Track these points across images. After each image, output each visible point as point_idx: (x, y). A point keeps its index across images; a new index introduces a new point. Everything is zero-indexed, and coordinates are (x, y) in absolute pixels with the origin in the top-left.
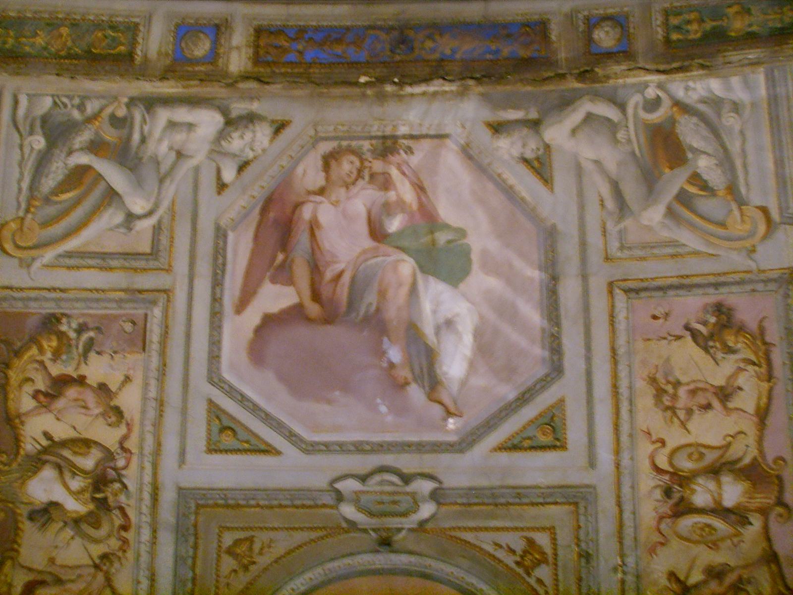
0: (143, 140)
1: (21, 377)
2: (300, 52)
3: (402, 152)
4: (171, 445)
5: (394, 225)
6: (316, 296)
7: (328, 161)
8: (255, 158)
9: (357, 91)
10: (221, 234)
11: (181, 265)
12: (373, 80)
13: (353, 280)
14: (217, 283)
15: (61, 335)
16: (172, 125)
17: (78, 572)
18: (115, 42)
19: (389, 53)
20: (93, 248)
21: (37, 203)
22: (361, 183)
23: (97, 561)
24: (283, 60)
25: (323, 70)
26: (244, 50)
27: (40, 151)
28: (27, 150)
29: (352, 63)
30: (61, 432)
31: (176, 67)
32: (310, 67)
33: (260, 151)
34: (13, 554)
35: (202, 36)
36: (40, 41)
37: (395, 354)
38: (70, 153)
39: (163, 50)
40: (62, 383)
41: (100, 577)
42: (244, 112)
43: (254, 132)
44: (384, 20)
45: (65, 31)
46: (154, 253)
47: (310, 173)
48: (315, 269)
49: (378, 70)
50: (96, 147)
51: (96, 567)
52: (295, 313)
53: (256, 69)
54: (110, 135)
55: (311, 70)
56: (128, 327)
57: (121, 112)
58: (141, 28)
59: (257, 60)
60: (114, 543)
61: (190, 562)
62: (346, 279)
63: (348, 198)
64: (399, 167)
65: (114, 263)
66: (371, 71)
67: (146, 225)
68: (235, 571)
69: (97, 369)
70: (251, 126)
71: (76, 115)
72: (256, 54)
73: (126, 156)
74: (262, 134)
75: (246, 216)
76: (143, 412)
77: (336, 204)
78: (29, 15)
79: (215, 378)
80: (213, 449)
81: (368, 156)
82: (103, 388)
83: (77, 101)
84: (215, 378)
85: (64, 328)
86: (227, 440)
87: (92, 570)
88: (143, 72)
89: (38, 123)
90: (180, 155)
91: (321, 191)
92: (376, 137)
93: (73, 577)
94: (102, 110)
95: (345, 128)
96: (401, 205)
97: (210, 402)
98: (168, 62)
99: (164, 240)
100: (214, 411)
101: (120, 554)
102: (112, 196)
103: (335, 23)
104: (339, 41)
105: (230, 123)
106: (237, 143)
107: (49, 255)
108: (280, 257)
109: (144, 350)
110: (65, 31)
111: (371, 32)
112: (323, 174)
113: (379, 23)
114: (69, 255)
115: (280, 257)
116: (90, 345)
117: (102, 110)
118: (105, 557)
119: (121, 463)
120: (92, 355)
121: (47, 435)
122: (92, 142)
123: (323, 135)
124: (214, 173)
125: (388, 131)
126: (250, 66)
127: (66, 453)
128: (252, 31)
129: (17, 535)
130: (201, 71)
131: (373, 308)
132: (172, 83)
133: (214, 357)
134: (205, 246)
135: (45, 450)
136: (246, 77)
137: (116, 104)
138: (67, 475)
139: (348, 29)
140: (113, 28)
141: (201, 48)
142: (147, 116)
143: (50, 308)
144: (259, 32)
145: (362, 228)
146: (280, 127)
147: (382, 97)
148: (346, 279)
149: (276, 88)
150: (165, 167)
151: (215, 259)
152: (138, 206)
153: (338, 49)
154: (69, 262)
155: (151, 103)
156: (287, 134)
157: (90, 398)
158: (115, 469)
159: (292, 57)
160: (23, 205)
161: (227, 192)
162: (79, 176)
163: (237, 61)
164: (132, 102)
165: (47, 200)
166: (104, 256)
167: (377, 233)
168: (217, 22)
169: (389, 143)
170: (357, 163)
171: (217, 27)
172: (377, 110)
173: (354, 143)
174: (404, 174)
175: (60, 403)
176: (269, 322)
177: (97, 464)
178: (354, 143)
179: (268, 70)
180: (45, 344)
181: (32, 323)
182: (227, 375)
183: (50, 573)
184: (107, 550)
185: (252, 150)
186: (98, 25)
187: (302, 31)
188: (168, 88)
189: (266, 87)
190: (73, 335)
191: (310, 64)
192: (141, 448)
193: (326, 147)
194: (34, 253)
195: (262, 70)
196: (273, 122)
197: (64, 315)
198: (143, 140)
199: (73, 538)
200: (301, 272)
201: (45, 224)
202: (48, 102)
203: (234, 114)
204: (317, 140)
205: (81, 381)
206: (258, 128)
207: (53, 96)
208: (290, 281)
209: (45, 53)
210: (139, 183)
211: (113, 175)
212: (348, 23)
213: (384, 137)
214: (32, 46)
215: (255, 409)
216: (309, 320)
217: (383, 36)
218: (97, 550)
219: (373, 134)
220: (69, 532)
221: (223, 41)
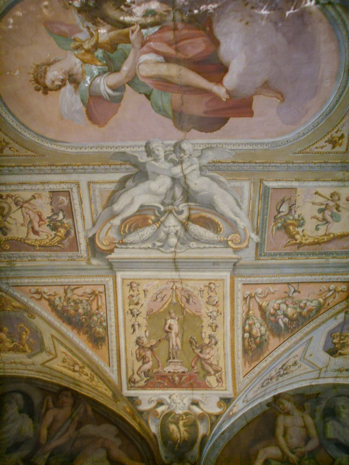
17: (25, 214)
23: (19, 207)
34: (22, 240)
41: (26, 205)
51: (21, 207)
60: (9, 200)
61: (10, 168)
68: (10, 148)
87: (23, 209)
93: (28, 216)
101: (14, 198)
118: (16, 204)
129: (14, 239)
183: (28, 225)
184: (13, 203)
199: (11, 217)
218: (14, 207)
220: (8, 219)
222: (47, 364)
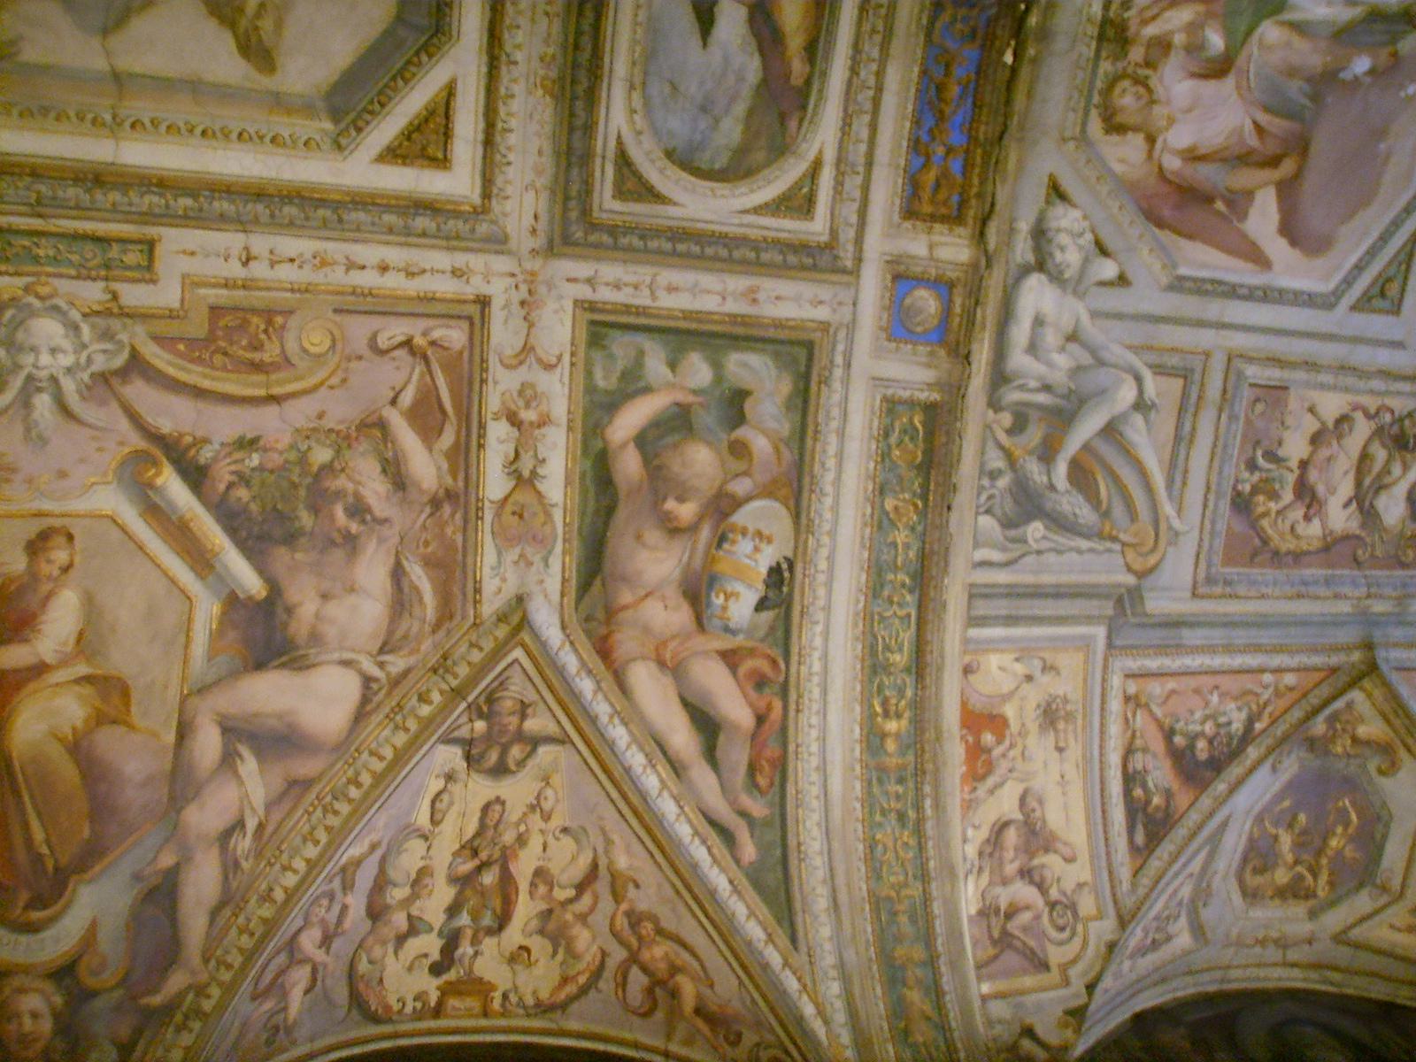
0: (1047, 388)
1: (1289, 537)
2: (950, 150)
3: (1126, 15)
4: (1384, 358)
5: (1216, 41)
6: (1274, 162)
7: (1115, 127)
8: (1093, 231)
9: (1025, 73)
10: (1179, 285)
11: (1206, 338)
12: (1013, 43)
13: (1267, 109)
14: (1232, 292)
15: (1255, 490)
16: (1033, 348)
18: (909, 431)
19: (975, 12)
20: (1167, 457)
21: (1107, 528)
22: (1153, 82)
24: (959, 179)
25: (984, 118)
26: (936, 238)
27: (1046, 527)
28: (1045, 545)
29: (978, 73)
30: (1346, 488)
31: (953, 341)
32: (976, 139)
33: (1086, 224)
35: (908, 301)
36: (901, 537)
37: (1361, 65)
38: (1052, 487)
39: (924, 360)
40: (1304, 491)
42: (1030, 242)
43: (1058, 230)
44: (921, 11)
45: (889, 504)
46: (1185, 374)
47: (1125, 154)
48: (1244, 159)
49: (999, 32)
50: (1047, 454)
52: (1287, 192)
53: (970, 221)
54: (1034, 434)
55: (981, 137)
56: (1260, 407)
57: (1006, 419)
58: (890, 392)
59: (956, 219)
62: (1263, 118)
63: (1168, 102)
64: (1145, 22)
65: (1187, 427)
66: (997, 43)
67: (1151, 384)
69: (1295, 447)
70: (1050, 234)
71: (1003, 482)
72: (944, 219)
73: (1063, 416)
74: (1065, 220)
75: (1163, 248)
76: (1347, 390)
77: (1171, 121)
78: (866, 555)
79: (1326, 303)
80: (1396, 310)
81: (1120, 65)
82: (1316, 440)
83: (986, 482)
84: (1326, 303)
85: (1247, 488)
86: (1393, 291)
88: (956, 390)
89: (1012, 533)
90: (1073, 337)
91: (1151, 140)
92: (1098, 51)
94: (1002, 447)
95: (1076, 95)
96: (1194, 28)
97: (1353, 308)
98: (942, 353)
99: (1174, 361)
100: (1363, 305)
102: (1111, 431)
103: (913, 90)
104: (940, 88)
105: (1041, 266)
106: (1069, 255)
107: (1168, 509)
108: (1220, 205)
109: (1286, 388)
110: (889, 504)
111: (937, 32)
112: (1130, 135)
113: (924, 21)
114: (1170, 483)
115: (1220, 205)
116: (1271, 456)
117: (1002, 447)
119: (1388, 418)
120: (1281, 453)
121: (1346, 505)
122: (1040, 459)
123: (1078, 129)
124: (1103, 290)
125: (1093, 31)
126: (960, 230)
127: (1367, 481)
128: (908, 224)
130: (963, 305)
131: (1307, 88)
132: (975, 347)
133: (1308, 300)
134: (1189, 305)
135: (1360, 508)
136: (981, 236)
137: (995, 426)
138: (1387, 480)
139: (924, 72)
140: (887, 435)
141: (927, 302)
142: (1016, 383)
143: (1225, 505)
144: (910, 213)
145: (1210, 86)
146: (1056, 192)
147: (1044, 34)
148: (1263, 118)
149: (1002, 195)
150: (1086, 359)
151: (1207, 293)
152: (1126, 394)
153: (954, 91)
154: (1178, 484)
155: (1000, 377)
156: (1068, 184)
157: (1324, 453)
158: (1392, 425)
159: (956, 166)
160: (1108, 544)
161: (1130, 275)
162: (1080, 475)
163: (954, 249)
164: (994, 404)
165: (1106, 515)
166: (1178, 438)
167: (1219, 68)
168: (889, 277)
169: (1111, 33)
170: (1126, 83)
171: (897, 277)
172: (1060, 44)
173: (1099, 84)
174: (1154, 18)
175: (1321, 489)
176: (1289, 229)
177: (1384, 445)
178: (1099, 84)
179: (973, 202)
180: (1260, 509)
181: (1239, 526)
182: (1331, 286)
185: (1081, 235)
186: (885, 456)
187: (916, 146)
188: (982, 354)
189: (998, 208)
190: (1256, 477)
191: (970, 137)
192: (1379, 394)
193: (1095, 126)
194: (1163, 526)
195: (971, 213)
196: (1048, 202)
197: (1234, 488)
198: (1047, 388)
200: (1244, 178)
201: (1133, 515)
202: (986, 521)
203: (1030, 258)
204: (1083, 139)
205: (1304, 465)
206: (1053, 224)
207: (977, 514)
208: (1249, 195)
209: (920, 528)
210: (1102, 393)
211: (1087, 428)
212: (916, 70)
213: (1101, 38)
214: (907, 546)
215: (1372, 253)
216: (1298, 175)
217: (945, 17)
219: (1092, 54)
221: (919, 269)
222: (1355, 933)
